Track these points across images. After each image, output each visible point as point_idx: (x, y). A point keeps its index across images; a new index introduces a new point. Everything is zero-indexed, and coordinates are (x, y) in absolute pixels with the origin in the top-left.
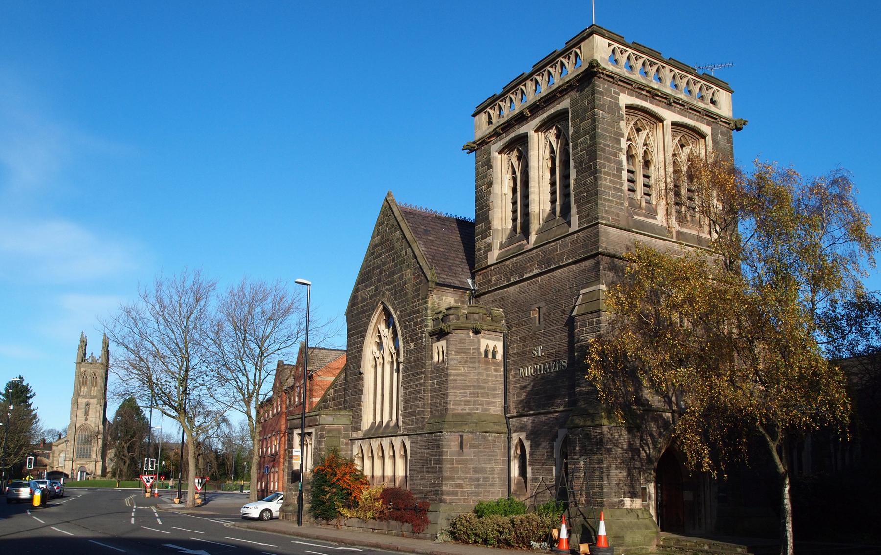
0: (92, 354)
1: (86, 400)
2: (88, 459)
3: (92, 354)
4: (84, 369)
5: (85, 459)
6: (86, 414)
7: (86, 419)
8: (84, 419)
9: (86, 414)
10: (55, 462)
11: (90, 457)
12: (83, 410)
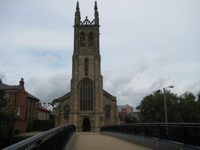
0: (87, 17)
1: (85, 57)
2: (91, 112)
3: (87, 17)
4: (81, 31)
5: (88, 112)
6: (86, 69)
7: (86, 74)
8: (84, 73)
9: (86, 69)
10: (61, 115)
11: (92, 109)
12: (83, 66)
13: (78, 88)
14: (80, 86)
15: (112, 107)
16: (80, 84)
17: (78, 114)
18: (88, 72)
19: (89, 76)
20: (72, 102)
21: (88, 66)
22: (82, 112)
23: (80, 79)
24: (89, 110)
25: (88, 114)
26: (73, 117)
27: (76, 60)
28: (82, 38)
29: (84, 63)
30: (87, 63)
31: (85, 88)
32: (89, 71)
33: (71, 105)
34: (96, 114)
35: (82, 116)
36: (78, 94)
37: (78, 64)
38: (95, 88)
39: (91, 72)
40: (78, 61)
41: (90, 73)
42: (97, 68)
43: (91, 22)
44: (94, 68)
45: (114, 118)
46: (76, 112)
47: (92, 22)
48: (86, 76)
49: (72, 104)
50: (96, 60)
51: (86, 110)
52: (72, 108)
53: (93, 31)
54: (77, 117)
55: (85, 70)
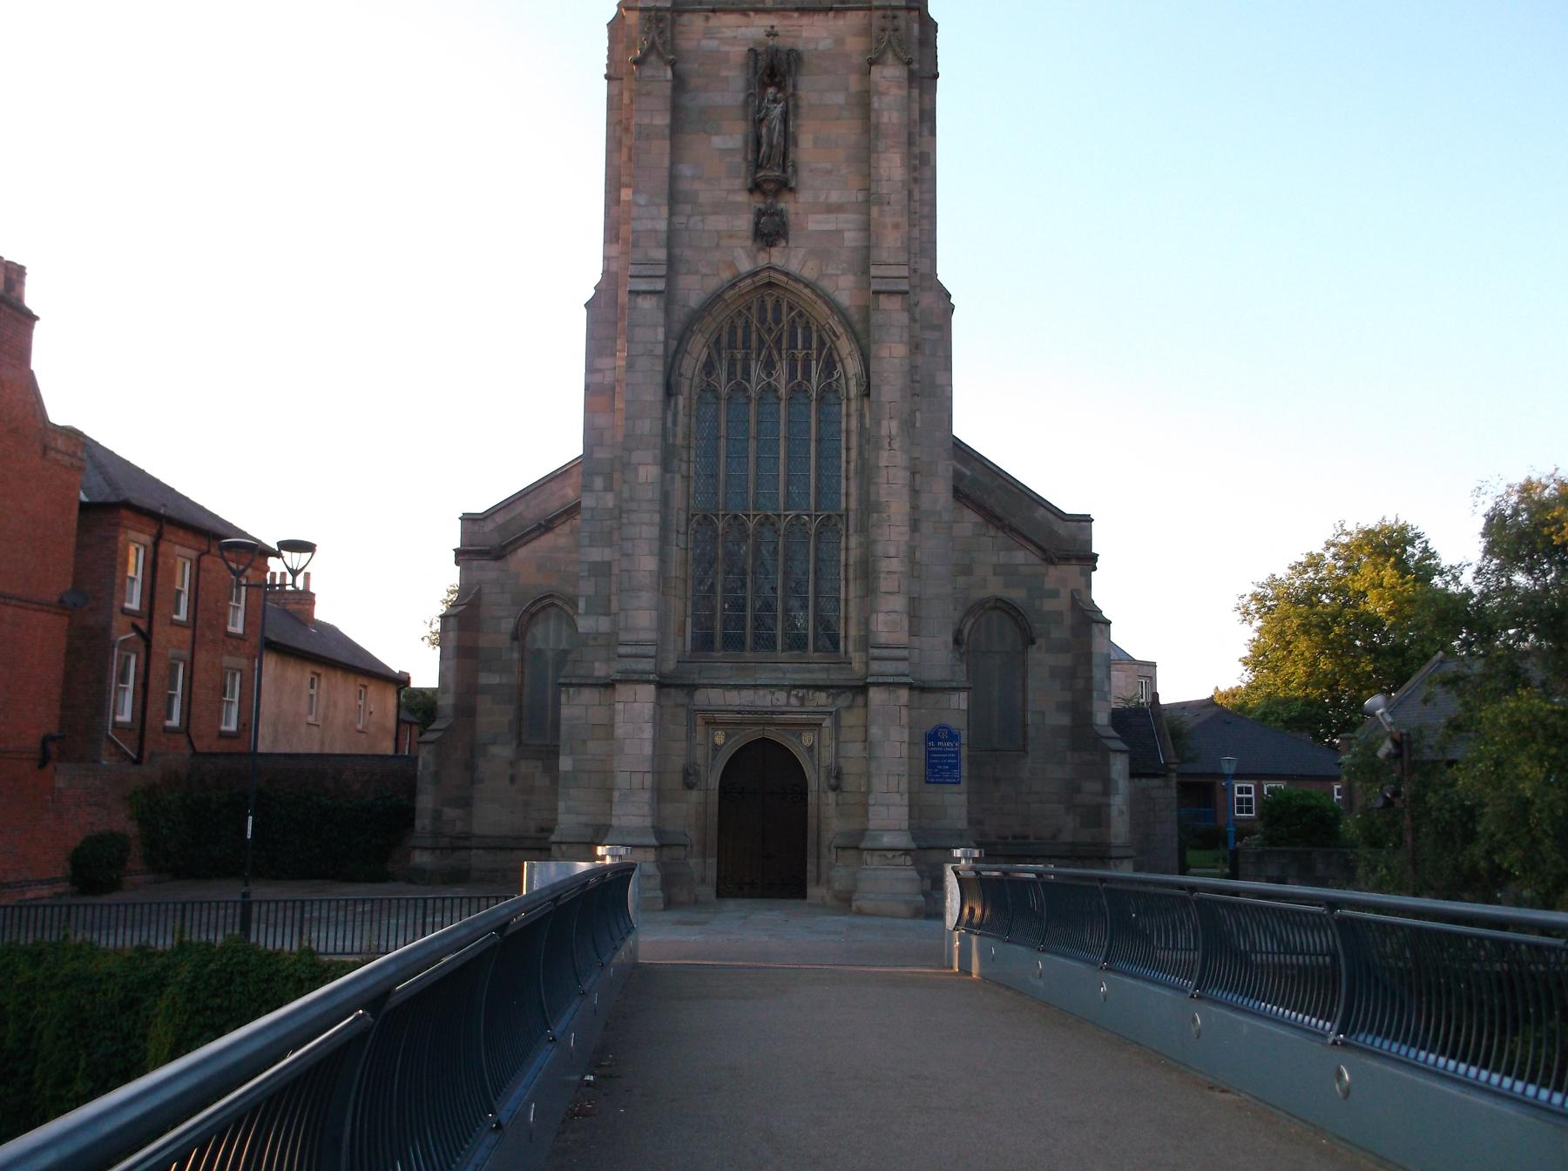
1: (755, 28)
7: (770, 231)
8: (744, 223)
11: (830, 639)
12: (731, 138)
13: (670, 390)
14: (691, 366)
16: (698, 348)
18: (786, 204)
19: (793, 259)
20: (597, 554)
21: (789, 139)
23: (694, 290)
25: (781, 696)
26: (610, 726)
29: (746, 104)
30: (777, 110)
32: (805, 196)
33: (587, 588)
34: (876, 696)
36: (666, 465)
37: (676, 110)
39: (831, 209)
40: (679, 84)
41: (817, 223)
42: (891, 165)
44: (865, 157)
46: (647, 665)
48: (763, 259)
49: (601, 570)
50: (889, 75)
52: (604, 624)
54: (659, 721)
55: (756, 188)
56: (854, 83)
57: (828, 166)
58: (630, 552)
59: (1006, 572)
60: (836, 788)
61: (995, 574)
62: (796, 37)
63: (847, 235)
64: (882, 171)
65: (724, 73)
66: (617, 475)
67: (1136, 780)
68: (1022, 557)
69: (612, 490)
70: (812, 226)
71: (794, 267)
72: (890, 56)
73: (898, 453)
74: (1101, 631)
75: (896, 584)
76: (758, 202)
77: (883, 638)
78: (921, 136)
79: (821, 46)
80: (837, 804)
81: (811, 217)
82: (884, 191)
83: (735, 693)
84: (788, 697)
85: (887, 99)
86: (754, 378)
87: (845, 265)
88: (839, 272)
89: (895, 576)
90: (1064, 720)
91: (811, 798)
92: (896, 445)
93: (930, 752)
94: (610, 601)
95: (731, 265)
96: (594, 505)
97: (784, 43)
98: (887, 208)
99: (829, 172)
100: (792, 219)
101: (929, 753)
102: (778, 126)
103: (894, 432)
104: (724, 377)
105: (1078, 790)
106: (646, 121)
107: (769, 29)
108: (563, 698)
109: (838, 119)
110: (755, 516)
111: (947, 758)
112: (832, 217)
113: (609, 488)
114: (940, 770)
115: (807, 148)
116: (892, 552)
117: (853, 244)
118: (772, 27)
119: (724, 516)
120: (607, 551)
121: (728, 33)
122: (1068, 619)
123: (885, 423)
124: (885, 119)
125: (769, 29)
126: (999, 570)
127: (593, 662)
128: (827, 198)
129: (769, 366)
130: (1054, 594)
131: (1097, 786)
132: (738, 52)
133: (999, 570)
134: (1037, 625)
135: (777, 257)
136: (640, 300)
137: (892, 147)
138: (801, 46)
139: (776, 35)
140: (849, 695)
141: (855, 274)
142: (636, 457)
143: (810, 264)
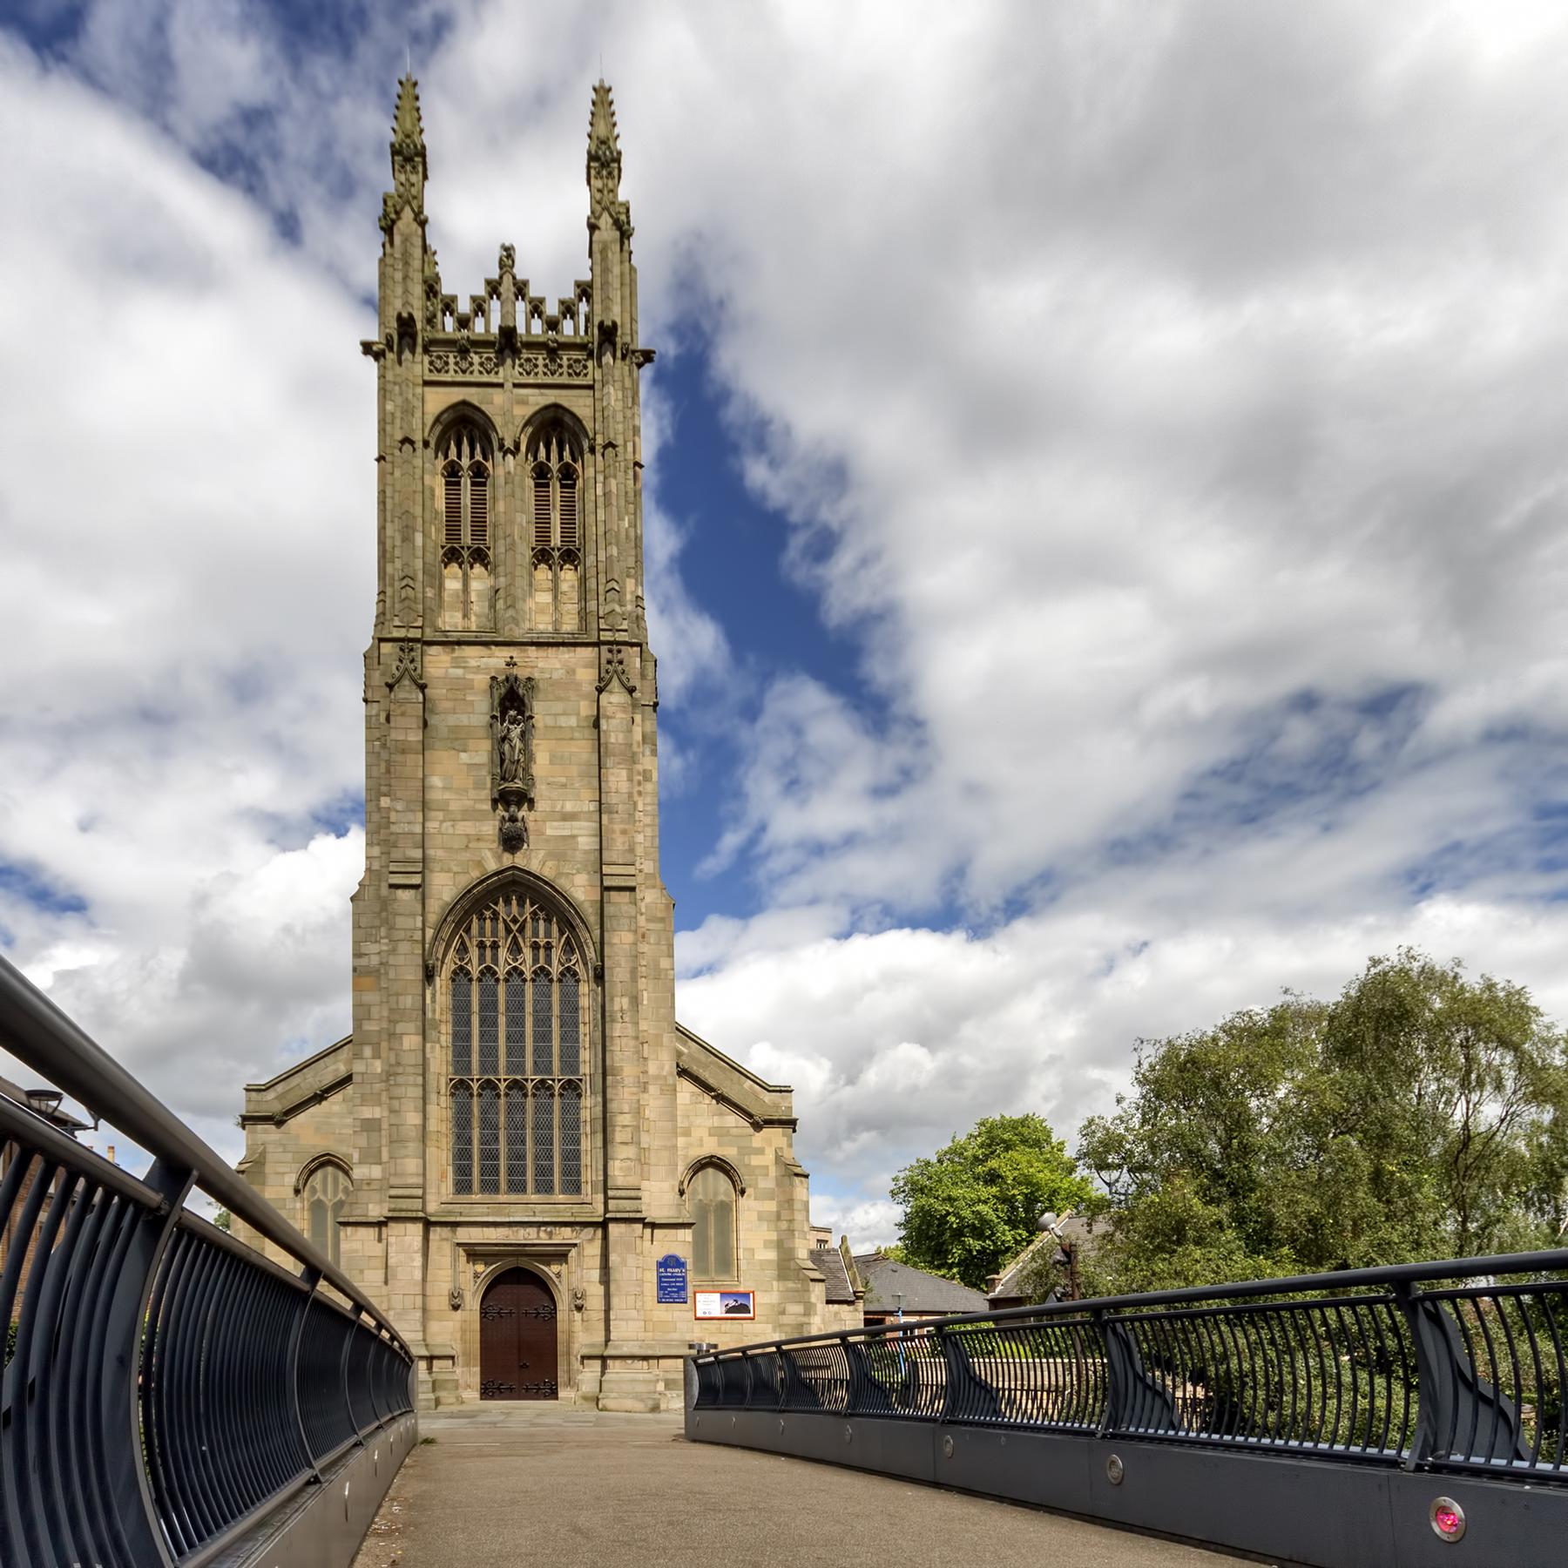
1: (497, 659)
2: (560, 1205)
5: (532, 1205)
7: (512, 840)
8: (490, 829)
11: (573, 1185)
12: (480, 752)
13: (429, 975)
15: (746, 1180)
17: (428, 1224)
19: (533, 859)
22: (479, 1206)
24: (545, 1187)
25: (532, 1231)
27: (407, 692)
28: (466, 482)
30: (516, 731)
31: (501, 971)
32: (541, 805)
34: (612, 1227)
35: (474, 1253)
38: (599, 977)
39: (567, 817)
43: (552, 309)
45: (772, 1273)
47: (568, 309)
48: (508, 860)
51: (517, 1187)
52: (376, 1172)
53: (579, 404)
56: (587, 709)
57: (563, 780)
58: (398, 1109)
59: (720, 1133)
60: (579, 1308)
61: (710, 1135)
62: (532, 667)
63: (580, 839)
64: (611, 784)
65: (469, 698)
66: (384, 1045)
67: (830, 1306)
68: (733, 1120)
69: (379, 1058)
70: (549, 832)
71: (534, 867)
72: (615, 683)
73: (629, 1025)
74: (801, 1182)
75: (630, 1136)
76: (501, 811)
77: (620, 1182)
78: (643, 755)
79: (556, 676)
80: (583, 1320)
81: (548, 824)
82: (614, 802)
83: (492, 1230)
84: (538, 1233)
85: (613, 722)
86: (501, 961)
87: (579, 866)
88: (574, 872)
89: (627, 1129)
90: (772, 1255)
91: (560, 1316)
92: (627, 1019)
93: (661, 1277)
94: (380, 1152)
95: (479, 864)
96: (364, 1071)
97: (522, 673)
98: (616, 816)
99: (564, 786)
100: (531, 826)
101: (660, 1278)
102: (518, 744)
103: (625, 1007)
104: (475, 961)
105: (783, 1313)
106: (401, 738)
107: (509, 660)
108: (342, 1234)
109: (572, 739)
110: (505, 1080)
111: (676, 1282)
112: (568, 824)
113: (376, 1056)
114: (670, 1292)
115: (541, 765)
116: (626, 1109)
117: (587, 848)
118: (512, 658)
119: (478, 1080)
120: (377, 1110)
121: (473, 663)
122: (773, 1171)
123: (617, 1000)
124: (613, 740)
125: (509, 660)
126: (713, 1132)
127: (367, 1204)
128: (562, 807)
129: (516, 949)
130: (761, 1151)
131: (799, 1309)
132: (482, 681)
133: (713, 1132)
134: (745, 1177)
135: (519, 860)
136: (400, 892)
137: (619, 763)
138: (536, 675)
139: (515, 664)
140: (591, 1230)
141: (589, 873)
142: (400, 1028)
143: (550, 864)
